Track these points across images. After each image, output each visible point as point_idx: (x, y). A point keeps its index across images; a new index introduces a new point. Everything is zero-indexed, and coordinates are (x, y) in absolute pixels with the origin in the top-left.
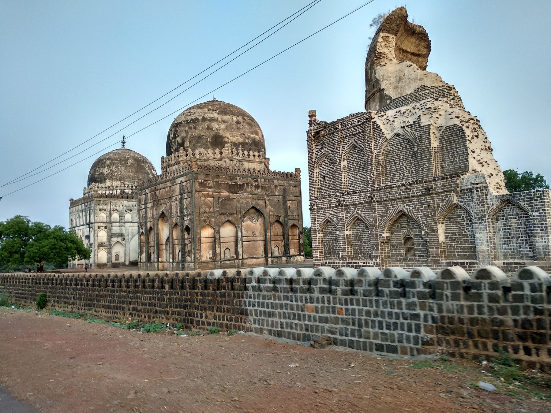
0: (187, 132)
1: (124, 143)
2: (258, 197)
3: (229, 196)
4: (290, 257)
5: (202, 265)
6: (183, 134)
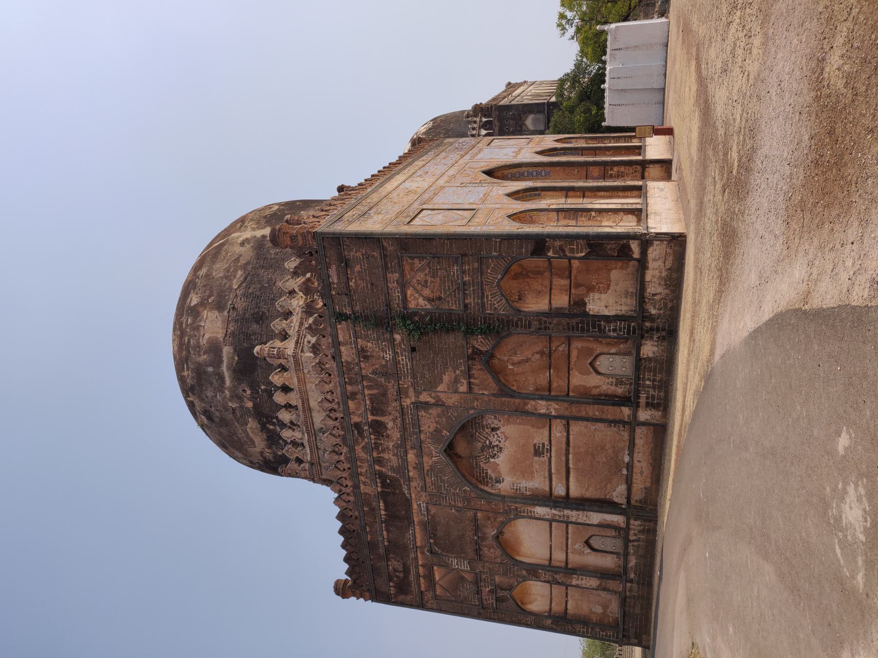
3: (424, 525)
4: (642, 313)
5: (632, 631)
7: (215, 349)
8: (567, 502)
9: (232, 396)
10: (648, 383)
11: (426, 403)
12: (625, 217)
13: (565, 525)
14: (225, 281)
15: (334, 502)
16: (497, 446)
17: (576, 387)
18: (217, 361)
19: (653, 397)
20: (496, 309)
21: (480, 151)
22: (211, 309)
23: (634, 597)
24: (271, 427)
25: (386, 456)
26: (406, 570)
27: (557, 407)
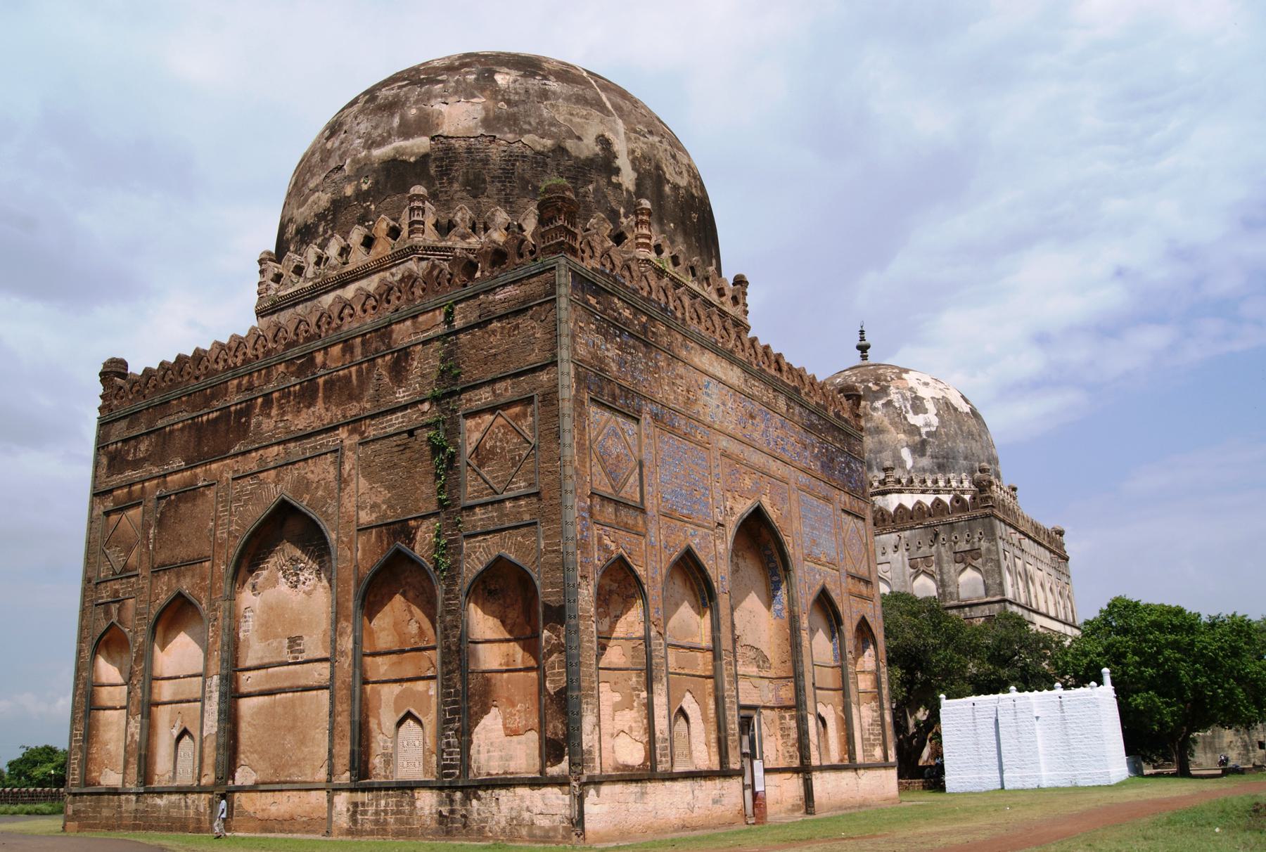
1: (863, 349)
2: (309, 443)
5: (80, 806)
7: (424, 125)
8: (232, 696)
9: (359, 161)
10: (383, 802)
11: (341, 464)
12: (641, 746)
13: (199, 695)
14: (533, 121)
15: (216, 343)
16: (298, 581)
17: (379, 693)
18: (406, 131)
19: (364, 813)
20: (469, 556)
21: (827, 499)
22: (486, 109)
23: (120, 806)
24: (321, 229)
25: (274, 412)
26: (136, 464)
27: (346, 666)
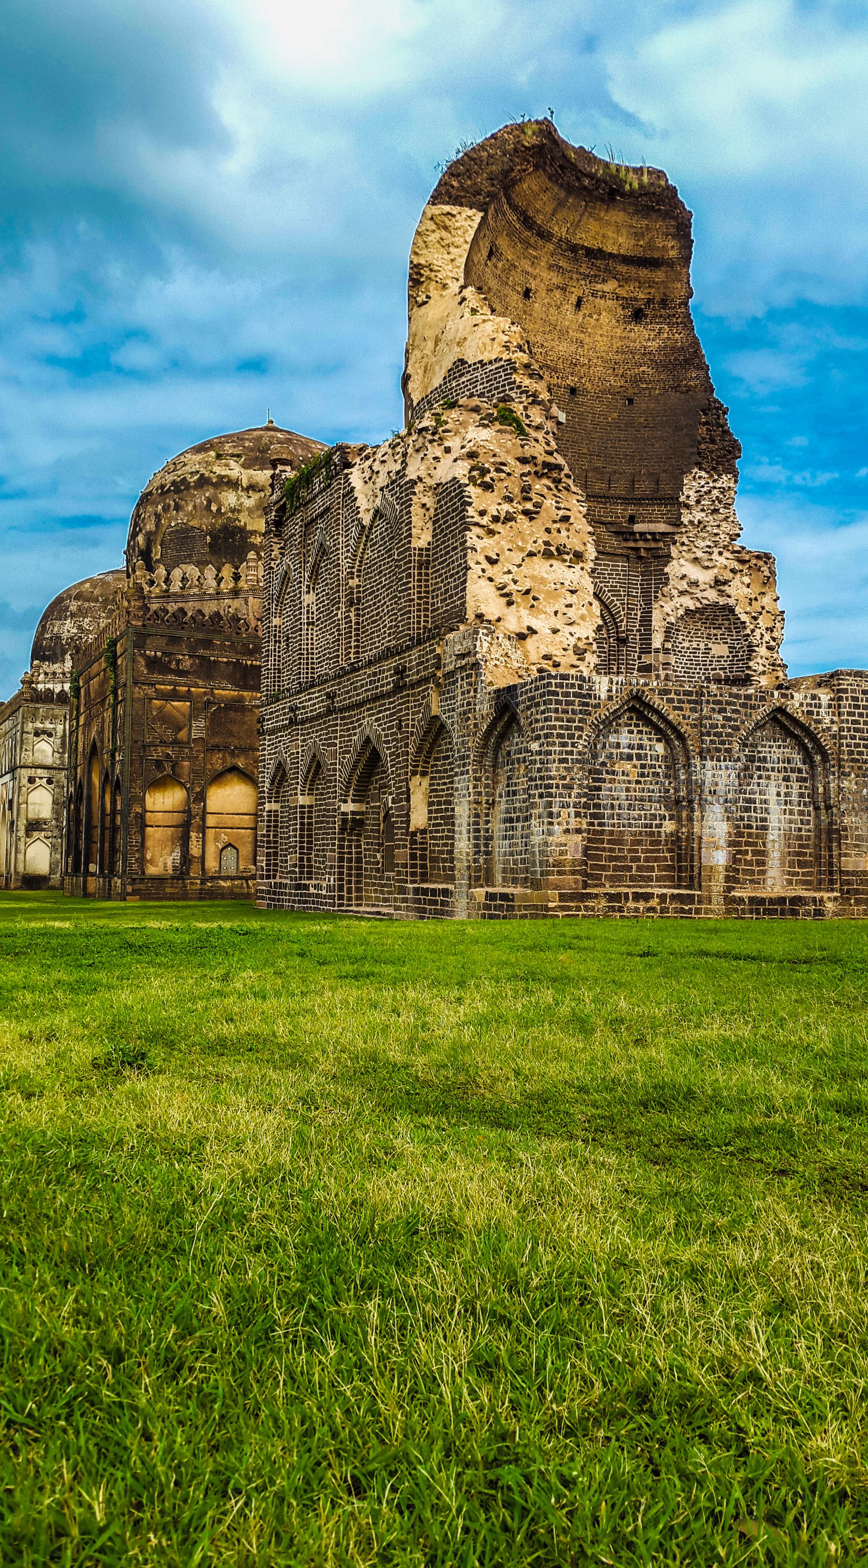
0: (158, 516)
3: (241, 699)
5: (142, 886)
6: (150, 526)
